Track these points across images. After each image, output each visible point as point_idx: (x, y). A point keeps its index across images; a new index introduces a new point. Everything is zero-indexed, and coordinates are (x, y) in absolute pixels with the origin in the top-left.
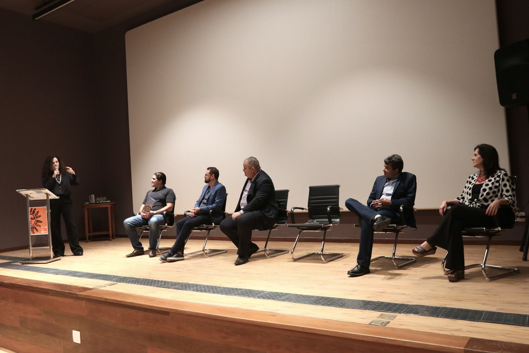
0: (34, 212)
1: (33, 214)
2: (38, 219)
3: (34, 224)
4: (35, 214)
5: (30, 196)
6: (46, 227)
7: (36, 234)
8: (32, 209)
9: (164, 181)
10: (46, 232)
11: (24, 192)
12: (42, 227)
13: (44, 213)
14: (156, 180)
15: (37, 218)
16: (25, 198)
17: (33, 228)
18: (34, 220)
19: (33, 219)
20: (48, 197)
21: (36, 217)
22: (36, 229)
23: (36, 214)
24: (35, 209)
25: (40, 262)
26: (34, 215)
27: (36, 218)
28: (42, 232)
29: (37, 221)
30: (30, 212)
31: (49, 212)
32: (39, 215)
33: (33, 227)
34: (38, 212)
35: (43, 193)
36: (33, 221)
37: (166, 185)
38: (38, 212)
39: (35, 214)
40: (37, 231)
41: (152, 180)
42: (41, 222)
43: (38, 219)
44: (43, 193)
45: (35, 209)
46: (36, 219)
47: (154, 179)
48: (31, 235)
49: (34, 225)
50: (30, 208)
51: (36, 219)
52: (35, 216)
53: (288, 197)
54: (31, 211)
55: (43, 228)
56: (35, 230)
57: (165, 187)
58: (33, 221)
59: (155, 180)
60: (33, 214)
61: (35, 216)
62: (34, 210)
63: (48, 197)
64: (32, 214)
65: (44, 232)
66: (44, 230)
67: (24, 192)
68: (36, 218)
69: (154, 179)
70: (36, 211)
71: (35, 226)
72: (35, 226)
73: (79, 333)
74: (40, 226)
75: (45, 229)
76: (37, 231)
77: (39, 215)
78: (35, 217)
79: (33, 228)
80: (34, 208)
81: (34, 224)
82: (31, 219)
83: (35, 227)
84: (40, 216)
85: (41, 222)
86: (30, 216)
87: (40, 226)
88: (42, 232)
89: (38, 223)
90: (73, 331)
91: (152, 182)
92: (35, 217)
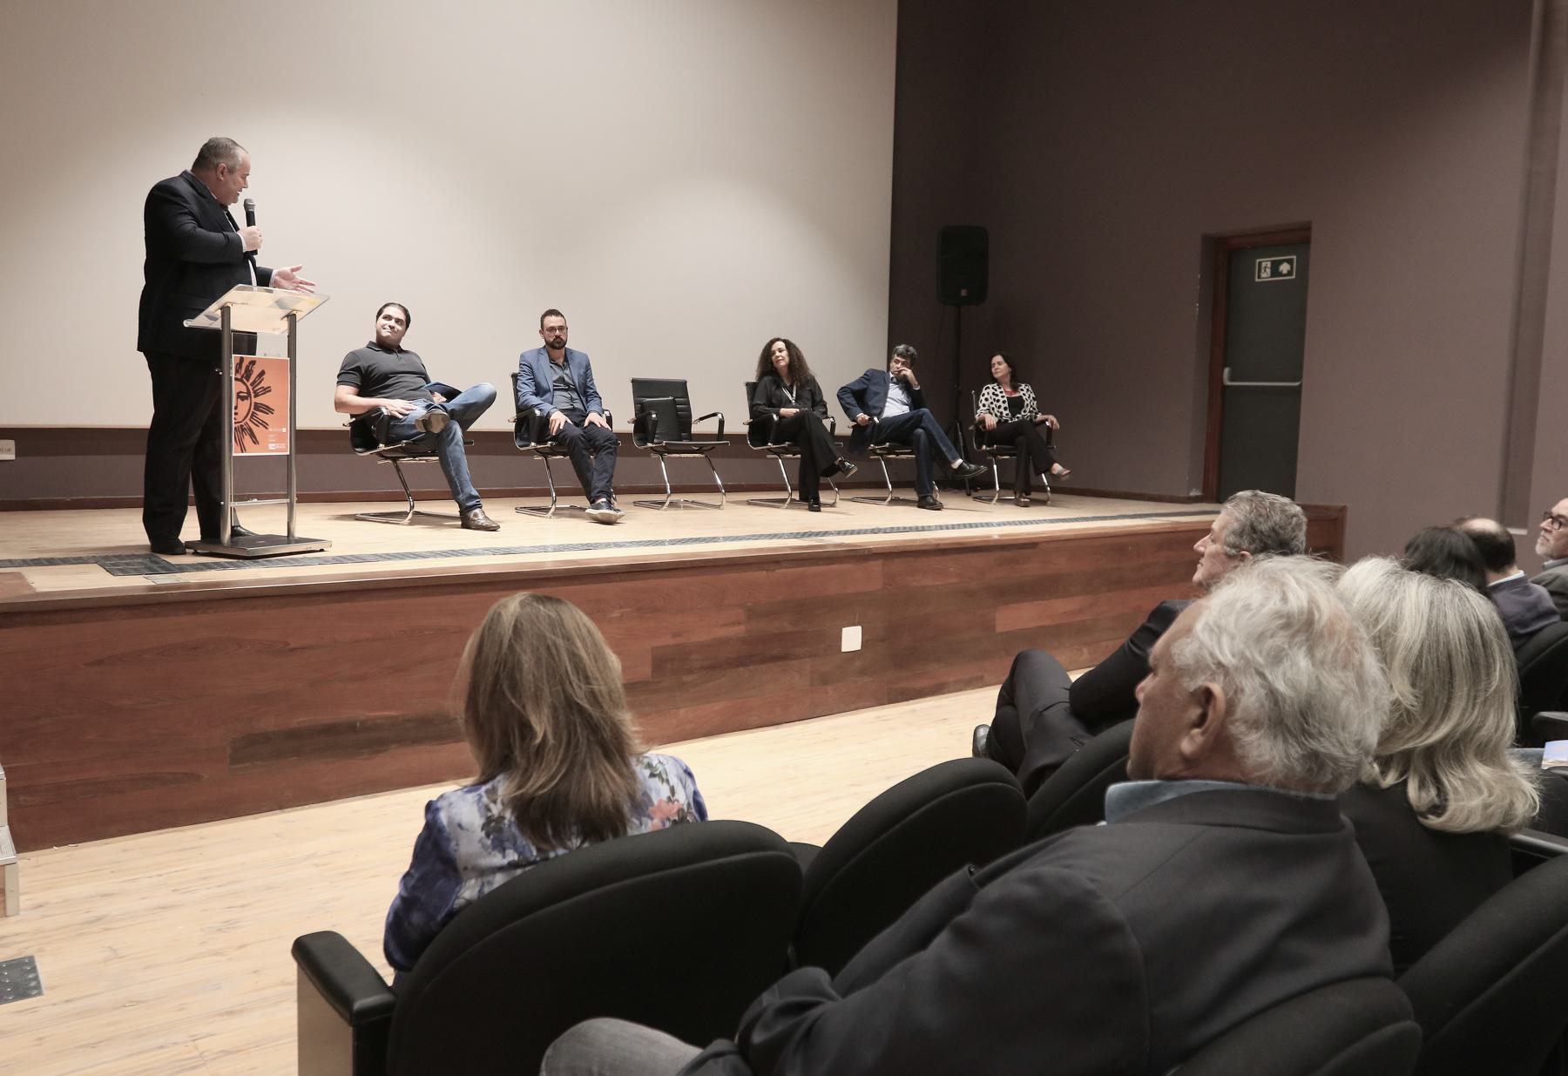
0: (248, 373)
1: (245, 380)
2: (259, 400)
3: (246, 416)
4: (251, 380)
6: (284, 430)
7: (252, 451)
8: (242, 359)
10: (283, 446)
12: (270, 430)
15: (256, 396)
17: (242, 429)
18: (247, 402)
19: (243, 399)
21: (255, 392)
22: (252, 435)
23: (255, 382)
24: (253, 363)
26: (248, 384)
27: (253, 395)
28: (271, 446)
29: (258, 407)
30: (237, 372)
33: (242, 426)
34: (263, 373)
36: (244, 407)
38: (263, 373)
39: (251, 380)
40: (256, 442)
42: (268, 410)
43: (259, 400)
45: (253, 363)
48: (234, 454)
49: (247, 420)
50: (235, 358)
51: (254, 400)
54: (241, 367)
55: (274, 433)
56: (247, 440)
58: (244, 407)
60: (245, 380)
61: (250, 388)
62: (247, 367)
64: (241, 380)
65: (278, 446)
68: (253, 395)
70: (256, 371)
73: (844, 629)
74: (265, 425)
76: (256, 442)
78: (252, 391)
79: (243, 430)
80: (248, 358)
81: (246, 416)
82: (238, 396)
83: (250, 429)
84: (267, 390)
85: (268, 410)
86: (237, 387)
87: (265, 425)
88: (271, 446)
89: (261, 415)
90: (859, 628)
92: (252, 391)
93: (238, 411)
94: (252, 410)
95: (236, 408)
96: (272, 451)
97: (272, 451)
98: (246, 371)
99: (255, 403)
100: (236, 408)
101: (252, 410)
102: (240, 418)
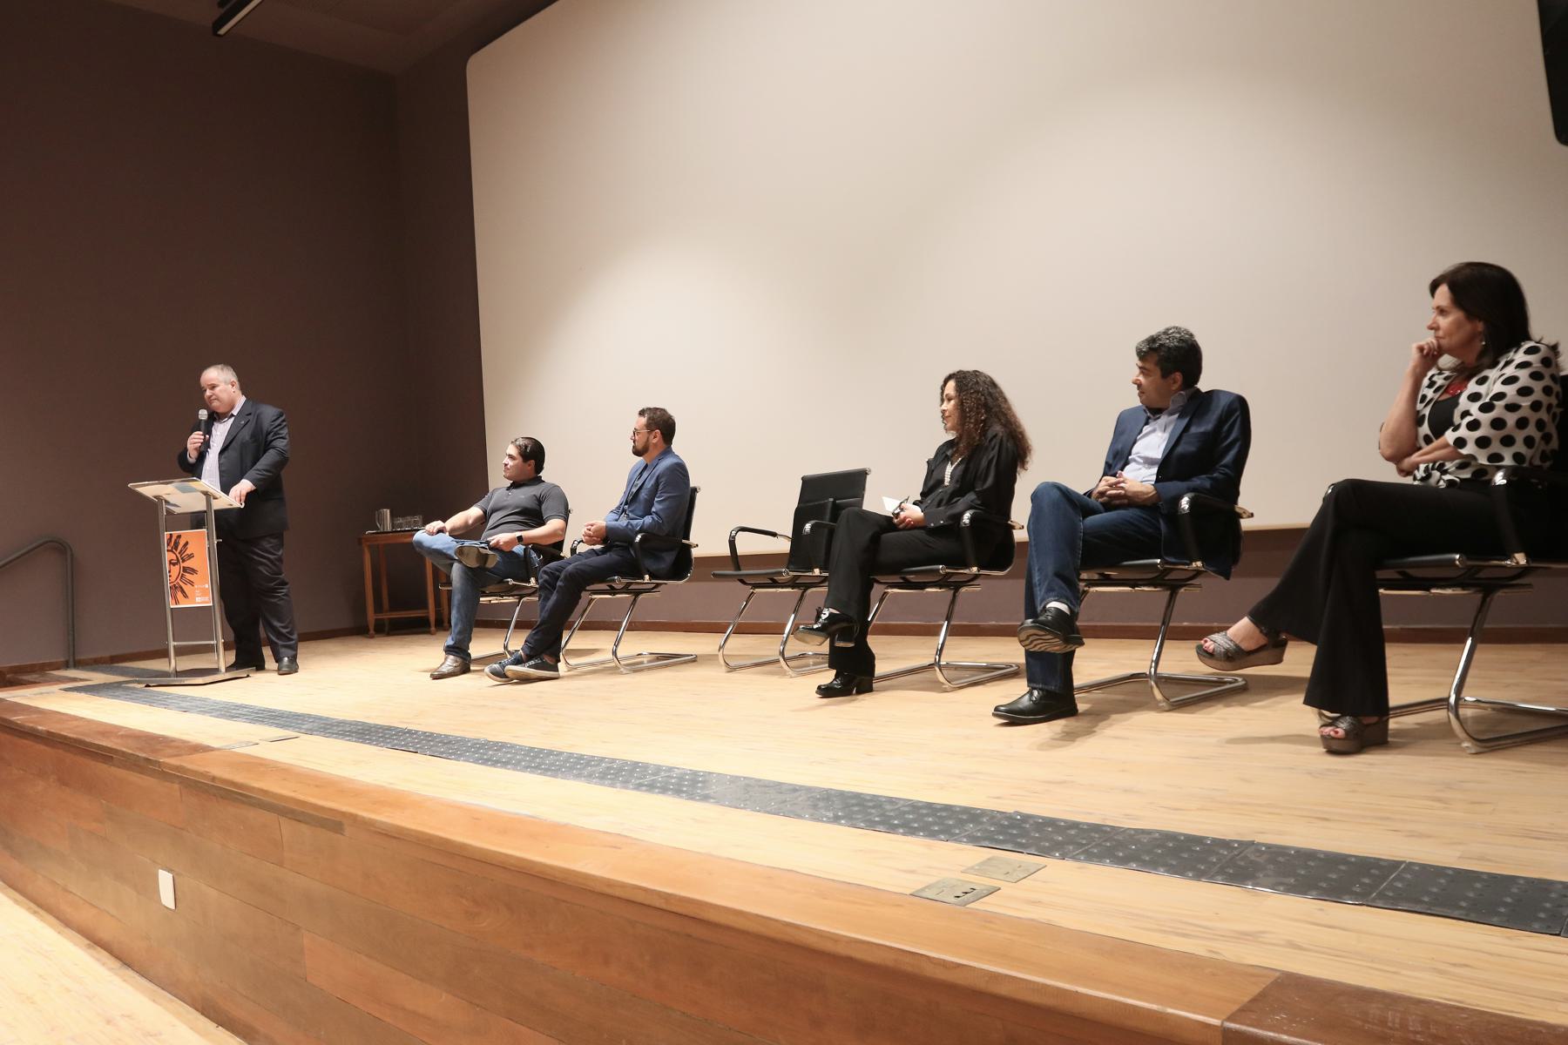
2: (186, 564)
4: (179, 550)
5: (167, 502)
6: (207, 586)
9: (539, 467)
11: (150, 490)
12: (196, 586)
13: (201, 546)
14: (520, 460)
15: (184, 561)
16: (154, 505)
17: (175, 588)
18: (177, 567)
19: (174, 564)
20: (209, 504)
22: (183, 591)
24: (179, 537)
25: (186, 683)
26: (177, 553)
27: (181, 561)
28: (198, 599)
29: (185, 569)
30: (168, 545)
31: (213, 543)
32: (188, 552)
34: (187, 543)
35: (195, 490)
36: (175, 570)
37: (544, 475)
38: (187, 543)
39: (179, 550)
40: (186, 596)
41: (507, 460)
42: (193, 571)
43: (186, 564)
44: (192, 490)
45: (179, 537)
46: (182, 565)
47: (511, 457)
49: (178, 580)
51: (182, 565)
52: (179, 556)
53: (864, 489)
56: (179, 595)
57: (539, 480)
58: (175, 570)
59: (516, 462)
61: (179, 556)
62: (176, 540)
63: (209, 504)
64: (171, 551)
66: (201, 594)
67: (150, 490)
68: (181, 561)
69: (511, 457)
70: (182, 543)
71: (181, 583)
72: (181, 583)
74: (192, 583)
75: (204, 593)
76: (186, 596)
77: (188, 552)
79: (176, 588)
82: (170, 563)
83: (181, 588)
84: (191, 556)
85: (193, 571)
86: (168, 556)
87: (192, 583)
88: (198, 599)
89: (188, 576)
91: (506, 465)
93: (172, 574)
94: (182, 572)
95: (170, 572)
96: (199, 603)
97: (199, 603)
98: (175, 542)
99: (184, 567)
100: (170, 572)
101: (182, 572)
102: (173, 579)
